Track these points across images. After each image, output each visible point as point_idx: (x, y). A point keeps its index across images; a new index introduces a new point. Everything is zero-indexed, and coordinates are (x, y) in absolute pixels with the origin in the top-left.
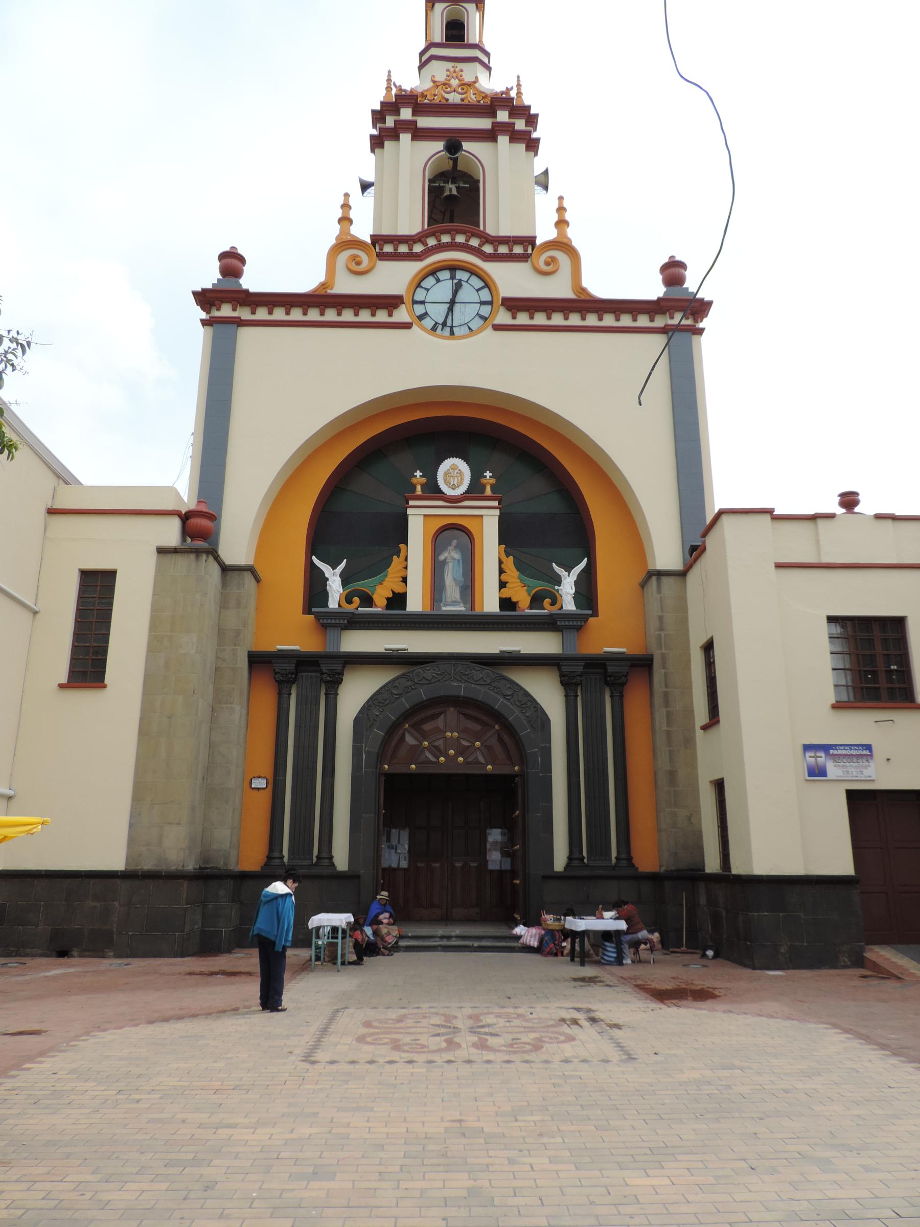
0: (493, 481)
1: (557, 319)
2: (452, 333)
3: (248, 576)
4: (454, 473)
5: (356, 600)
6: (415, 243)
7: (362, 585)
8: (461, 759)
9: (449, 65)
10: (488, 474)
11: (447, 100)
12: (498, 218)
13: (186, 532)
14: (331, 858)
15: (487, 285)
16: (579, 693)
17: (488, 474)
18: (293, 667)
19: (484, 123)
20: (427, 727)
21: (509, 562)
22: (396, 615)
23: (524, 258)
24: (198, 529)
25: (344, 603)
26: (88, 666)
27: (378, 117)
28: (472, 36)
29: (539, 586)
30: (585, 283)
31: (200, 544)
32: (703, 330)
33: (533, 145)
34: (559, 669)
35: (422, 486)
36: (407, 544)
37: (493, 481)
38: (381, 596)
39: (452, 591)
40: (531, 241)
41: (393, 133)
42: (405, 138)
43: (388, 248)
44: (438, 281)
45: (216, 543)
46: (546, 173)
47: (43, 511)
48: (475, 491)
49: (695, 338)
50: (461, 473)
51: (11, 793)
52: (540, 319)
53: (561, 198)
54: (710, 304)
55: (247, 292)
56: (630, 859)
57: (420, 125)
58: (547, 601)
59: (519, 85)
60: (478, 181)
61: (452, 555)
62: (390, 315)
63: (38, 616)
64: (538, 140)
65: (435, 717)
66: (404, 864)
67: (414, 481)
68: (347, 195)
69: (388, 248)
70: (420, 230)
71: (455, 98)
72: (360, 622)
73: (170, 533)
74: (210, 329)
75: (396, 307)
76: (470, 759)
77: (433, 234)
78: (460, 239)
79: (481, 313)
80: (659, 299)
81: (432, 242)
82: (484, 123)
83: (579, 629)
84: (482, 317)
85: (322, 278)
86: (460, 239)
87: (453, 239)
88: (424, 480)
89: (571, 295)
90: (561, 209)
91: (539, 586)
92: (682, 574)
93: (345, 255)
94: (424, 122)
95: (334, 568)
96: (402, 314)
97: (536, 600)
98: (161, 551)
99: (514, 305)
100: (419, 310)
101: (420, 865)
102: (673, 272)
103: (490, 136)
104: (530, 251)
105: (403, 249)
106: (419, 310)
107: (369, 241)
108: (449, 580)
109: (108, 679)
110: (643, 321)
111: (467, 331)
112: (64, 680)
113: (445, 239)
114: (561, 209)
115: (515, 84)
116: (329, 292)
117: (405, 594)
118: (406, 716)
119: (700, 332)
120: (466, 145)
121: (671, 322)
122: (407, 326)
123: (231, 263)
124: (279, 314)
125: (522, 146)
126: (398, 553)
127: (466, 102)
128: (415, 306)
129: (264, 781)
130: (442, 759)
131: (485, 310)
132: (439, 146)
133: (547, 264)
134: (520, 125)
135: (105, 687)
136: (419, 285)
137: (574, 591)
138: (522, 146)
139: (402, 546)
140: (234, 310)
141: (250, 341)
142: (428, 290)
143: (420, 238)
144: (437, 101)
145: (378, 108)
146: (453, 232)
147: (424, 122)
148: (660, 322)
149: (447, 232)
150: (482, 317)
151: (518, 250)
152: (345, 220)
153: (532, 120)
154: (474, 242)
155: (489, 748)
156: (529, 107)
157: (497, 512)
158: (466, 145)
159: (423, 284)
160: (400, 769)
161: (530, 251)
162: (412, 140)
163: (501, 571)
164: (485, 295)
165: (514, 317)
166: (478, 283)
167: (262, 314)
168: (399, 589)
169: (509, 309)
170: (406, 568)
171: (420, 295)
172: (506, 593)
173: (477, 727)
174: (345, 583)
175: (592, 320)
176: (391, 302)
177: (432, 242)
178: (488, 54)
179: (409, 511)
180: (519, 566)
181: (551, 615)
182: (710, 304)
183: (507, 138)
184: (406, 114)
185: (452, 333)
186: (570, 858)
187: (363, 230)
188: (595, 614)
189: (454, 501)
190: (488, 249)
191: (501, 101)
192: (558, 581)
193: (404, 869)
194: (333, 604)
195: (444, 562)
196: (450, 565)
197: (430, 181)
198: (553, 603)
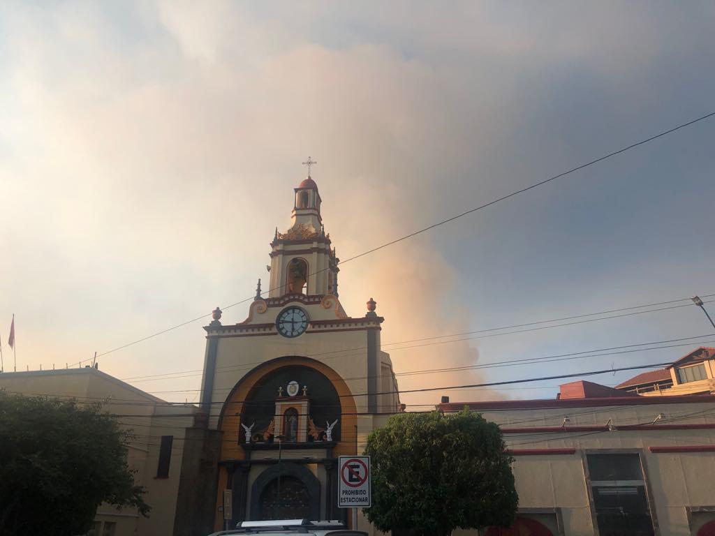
4: (293, 388)
5: (257, 439)
10: (305, 387)
13: (196, 421)
17: (305, 387)
23: (318, 302)
24: (200, 417)
25: (252, 439)
27: (273, 245)
28: (310, 204)
39: (293, 433)
42: (281, 256)
43: (271, 303)
52: (323, 328)
55: (222, 326)
62: (270, 330)
68: (260, 280)
73: (190, 422)
81: (287, 299)
83: (333, 447)
85: (247, 317)
86: (297, 297)
93: (256, 306)
96: (275, 330)
98: (188, 429)
99: (314, 323)
100: (281, 326)
102: (372, 305)
105: (277, 303)
106: (281, 326)
109: (169, 475)
110: (359, 326)
112: (155, 475)
113: (292, 297)
119: (380, 329)
121: (368, 326)
122: (276, 334)
123: (217, 314)
126: (273, 419)
133: (328, 304)
134: (323, 246)
136: (281, 315)
141: (222, 342)
143: (282, 298)
146: (294, 295)
151: (317, 300)
152: (259, 290)
154: (301, 298)
163: (308, 425)
165: (313, 327)
167: (227, 333)
171: (282, 319)
175: (341, 327)
176: (270, 326)
179: (276, 403)
180: (314, 422)
183: (316, 253)
190: (306, 300)
192: (327, 429)
195: (291, 421)
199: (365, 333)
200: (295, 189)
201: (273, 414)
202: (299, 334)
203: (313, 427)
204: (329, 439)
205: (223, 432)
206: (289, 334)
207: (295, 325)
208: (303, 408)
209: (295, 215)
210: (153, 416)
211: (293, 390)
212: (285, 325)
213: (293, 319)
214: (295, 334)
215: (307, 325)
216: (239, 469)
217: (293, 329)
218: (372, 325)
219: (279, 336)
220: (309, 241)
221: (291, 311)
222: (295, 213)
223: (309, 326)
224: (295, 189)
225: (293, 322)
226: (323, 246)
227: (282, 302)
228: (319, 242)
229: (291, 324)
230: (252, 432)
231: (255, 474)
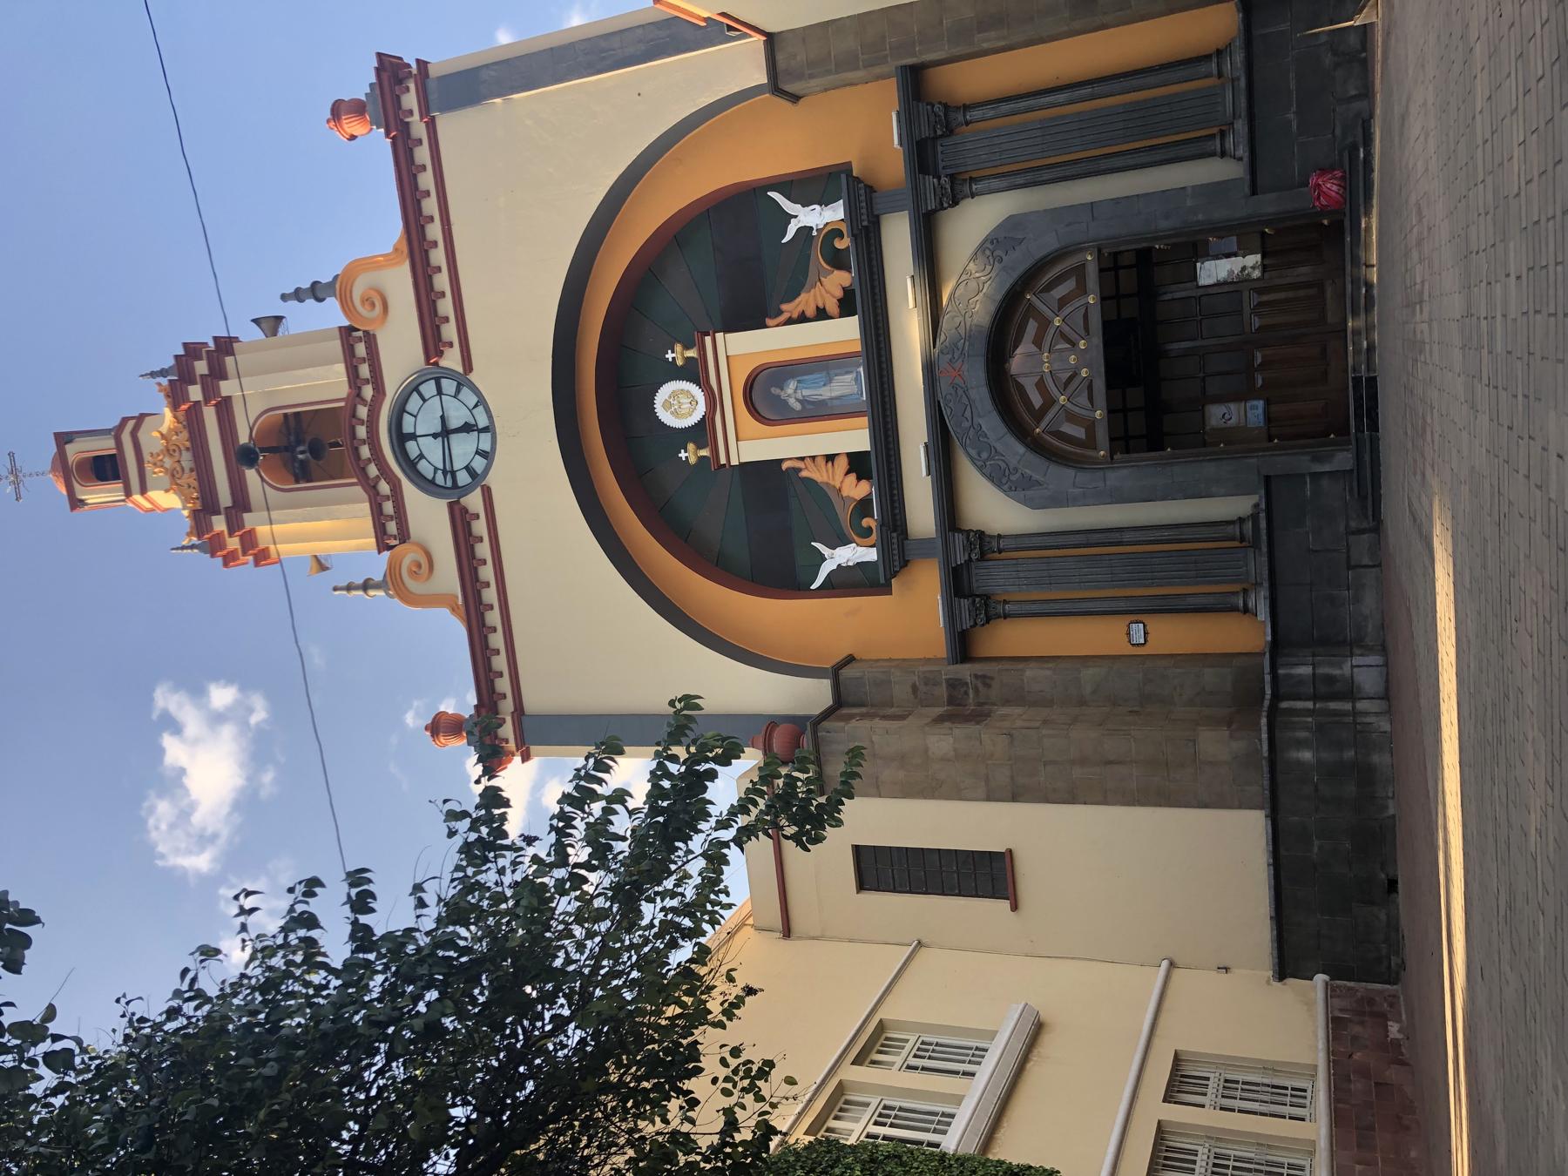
0: (678, 347)
1: (442, 281)
2: (485, 430)
3: (846, 673)
4: (677, 405)
5: (866, 522)
6: (378, 493)
7: (845, 516)
8: (1082, 344)
9: (148, 467)
11: (192, 470)
12: (326, 383)
14: (1241, 520)
15: (416, 389)
16: (967, 176)
18: (965, 603)
19: (210, 415)
20: (1037, 400)
21: (790, 309)
22: (879, 464)
23: (370, 340)
26: (987, 875)
27: (229, 559)
28: (106, 446)
29: (818, 258)
30: (390, 250)
31: (806, 741)
32: (418, 61)
33: (226, 345)
34: (934, 211)
35: (700, 447)
36: (780, 461)
37: (678, 347)
38: (855, 489)
40: (347, 333)
41: (249, 540)
43: (392, 527)
44: (421, 456)
45: (806, 718)
46: (255, 321)
47: (788, 942)
48: (694, 372)
49: (433, 72)
50: (674, 394)
51: (1165, 964)
52: (446, 307)
53: (284, 297)
54: (379, 55)
56: (1219, 52)
57: (229, 504)
58: (841, 244)
59: (153, 374)
60: (286, 415)
61: (792, 392)
63: (924, 941)
64: (216, 339)
65: (1020, 388)
66: (1260, 404)
67: (693, 460)
69: (392, 527)
70: (359, 489)
71: (187, 460)
72: (894, 515)
74: (533, 749)
75: (465, 510)
76: (1083, 333)
77: (364, 469)
78: (362, 432)
79: (452, 391)
80: (387, 134)
81: (373, 470)
82: (210, 415)
83: (870, 189)
84: (458, 391)
85: (445, 612)
86: (362, 432)
87: (364, 442)
88: (691, 446)
89: (406, 268)
90: (298, 295)
91: (818, 258)
92: (771, 39)
93: (412, 585)
94: (225, 497)
95: (823, 559)
96: (474, 501)
97: (837, 261)
99: (433, 344)
100: (463, 478)
101: (1260, 382)
103: (225, 409)
104: (360, 334)
105: (388, 508)
106: (463, 478)
107: (387, 554)
108: (826, 393)
110: (423, 154)
111: (481, 408)
112: (1006, 904)
114: (298, 295)
115: (153, 381)
116: (460, 601)
117: (848, 455)
118: (1020, 430)
120: (243, 439)
121: (416, 116)
122: (487, 494)
124: (500, 663)
125: (229, 360)
127: (188, 444)
128: (460, 484)
129: (1134, 626)
130: (1084, 373)
131: (449, 386)
132: (251, 475)
133: (373, 305)
134: (201, 367)
135: (1010, 851)
136: (432, 482)
137: (817, 207)
138: (229, 360)
139: (785, 466)
140: (504, 721)
142: (436, 469)
144: (195, 484)
145: (220, 560)
147: (225, 497)
148: (419, 129)
149: (356, 450)
150: (458, 391)
151: (361, 350)
152: (366, 586)
153: (192, 351)
154: (363, 412)
155: (1063, 302)
156: (177, 357)
157: (719, 336)
158: (243, 439)
159: (430, 477)
160: (1102, 435)
161: (360, 334)
162: (249, 510)
163: (803, 318)
164: (429, 389)
165: (451, 345)
166: (414, 403)
167: (503, 685)
168: (842, 464)
169: (440, 354)
170: (813, 458)
172: (832, 306)
173: (1032, 327)
174: (843, 541)
175: (434, 231)
176: (461, 521)
177: (373, 470)
178: (125, 420)
179: (734, 462)
180: (792, 295)
181: (854, 236)
182: (379, 55)
184: (219, 524)
185: (485, 430)
186: (1223, 154)
187: (378, 565)
188: (846, 168)
189: (713, 401)
190: (368, 391)
191: (176, 396)
192: (805, 231)
193: (1268, 403)
194: (871, 555)
195: (802, 402)
196: (806, 392)
197: (297, 482)
198: (838, 233)
199: (448, 124)
200: (73, 508)
201: (771, 468)
202: (481, 401)
203: (806, 301)
204: (835, 213)
205: (850, 659)
206: (485, 445)
207: (454, 423)
208: (743, 349)
209: (143, 491)
210: (787, 932)
211: (685, 400)
212: (459, 464)
213: (435, 436)
214: (483, 422)
215: (450, 375)
216: (975, 576)
217: (467, 428)
218: (410, 100)
219: (492, 480)
220: (192, 422)
221: (412, 447)
222: (137, 497)
223: (444, 363)
224: (73, 508)
225: (445, 433)
226: (201, 367)
227: (384, 488)
228: (194, 383)
229: (453, 437)
230: (840, 540)
231: (992, 508)
